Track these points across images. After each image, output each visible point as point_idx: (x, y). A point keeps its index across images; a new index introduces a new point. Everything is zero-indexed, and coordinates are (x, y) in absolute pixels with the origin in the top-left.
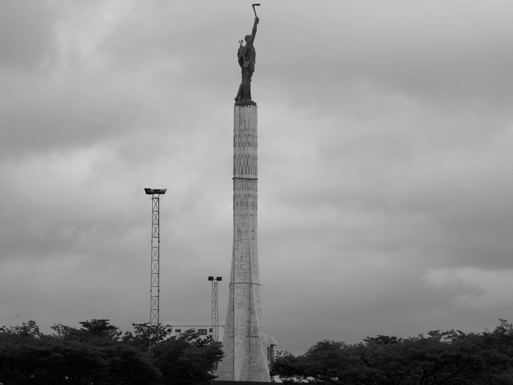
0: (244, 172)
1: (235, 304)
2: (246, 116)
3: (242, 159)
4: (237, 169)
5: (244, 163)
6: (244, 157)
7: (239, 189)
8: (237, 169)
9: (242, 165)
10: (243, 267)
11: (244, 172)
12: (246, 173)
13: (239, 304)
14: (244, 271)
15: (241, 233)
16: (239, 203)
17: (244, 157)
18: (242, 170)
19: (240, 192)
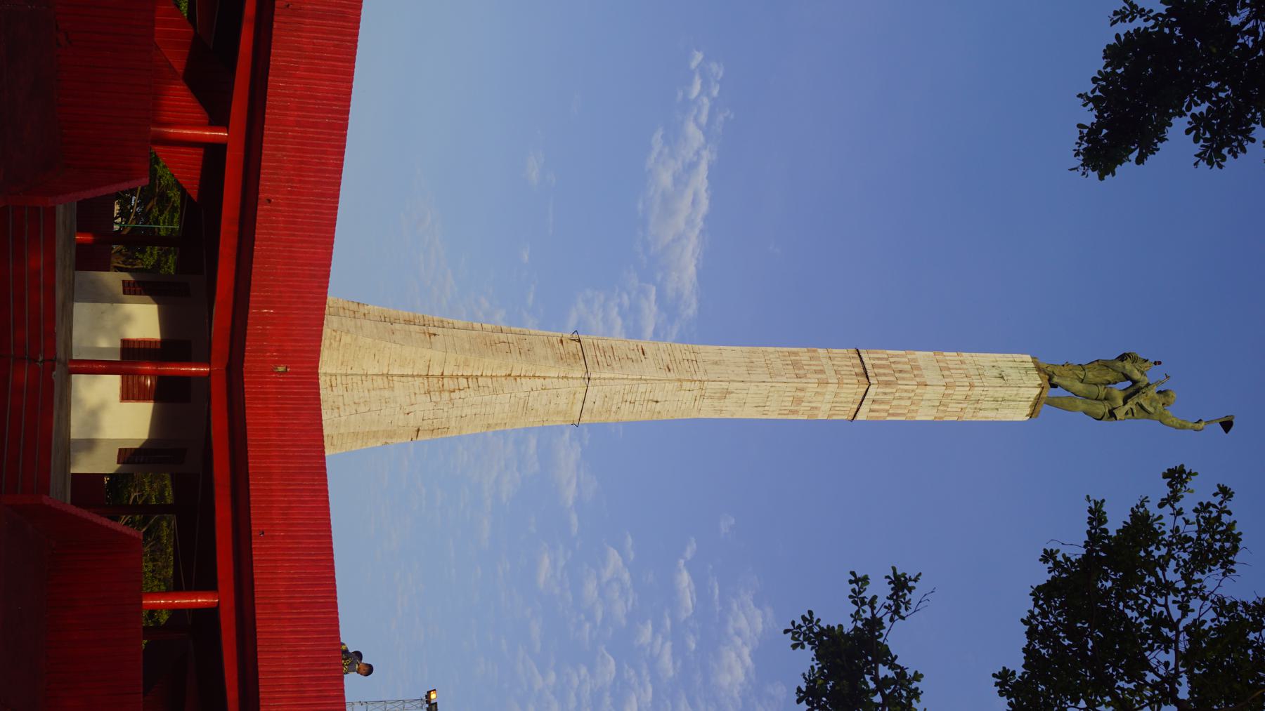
0: (875, 407)
1: (527, 384)
2: (1006, 411)
3: (909, 402)
4: (887, 390)
5: (898, 407)
6: (913, 407)
7: (836, 394)
8: (887, 390)
9: (895, 403)
10: (626, 408)
11: (875, 407)
12: (871, 411)
13: (526, 403)
14: (614, 408)
15: (720, 398)
16: (800, 394)
17: (913, 407)
18: (882, 402)
19: (829, 397)
